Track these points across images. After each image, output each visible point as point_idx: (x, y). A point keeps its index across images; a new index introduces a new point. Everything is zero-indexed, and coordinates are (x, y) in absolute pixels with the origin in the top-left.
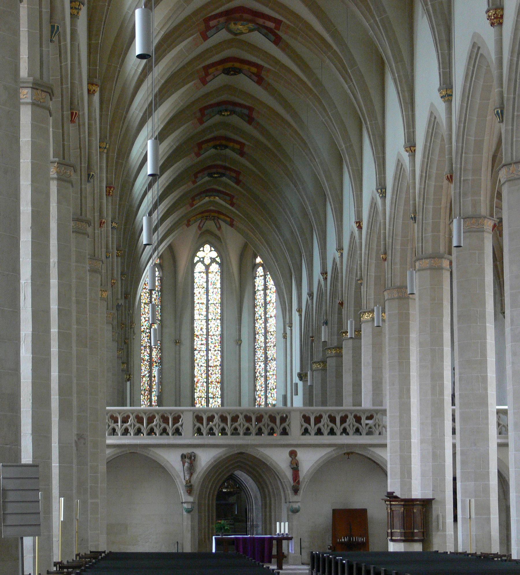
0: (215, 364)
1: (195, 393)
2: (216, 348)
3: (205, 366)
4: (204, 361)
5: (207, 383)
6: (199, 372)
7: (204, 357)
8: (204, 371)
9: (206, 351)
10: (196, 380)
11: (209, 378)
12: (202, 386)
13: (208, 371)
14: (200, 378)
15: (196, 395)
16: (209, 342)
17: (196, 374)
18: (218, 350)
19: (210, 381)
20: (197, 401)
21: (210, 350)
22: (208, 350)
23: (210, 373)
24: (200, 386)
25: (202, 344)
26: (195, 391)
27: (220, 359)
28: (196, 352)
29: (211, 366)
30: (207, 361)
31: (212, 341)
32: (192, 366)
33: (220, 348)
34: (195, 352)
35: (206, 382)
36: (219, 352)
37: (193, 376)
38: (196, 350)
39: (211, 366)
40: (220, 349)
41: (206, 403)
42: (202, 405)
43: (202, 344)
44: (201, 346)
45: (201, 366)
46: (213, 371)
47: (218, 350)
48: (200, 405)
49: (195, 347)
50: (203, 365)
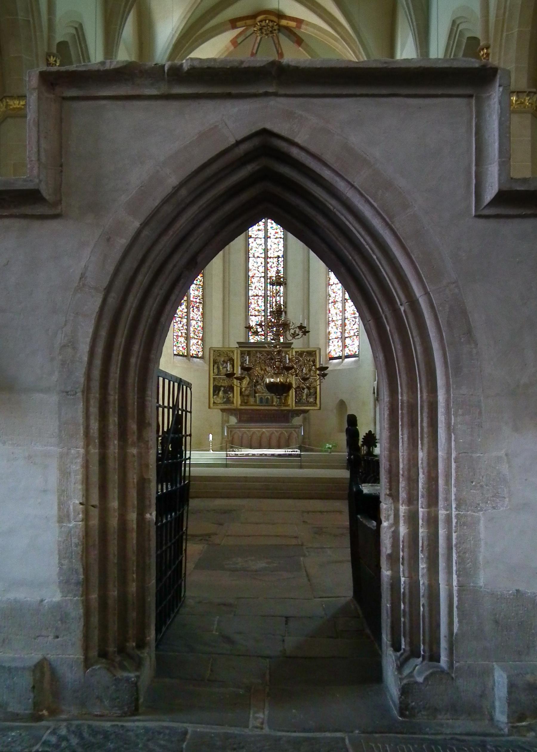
0: (276, 254)
1: (250, 291)
2: (277, 235)
3: (264, 257)
4: (262, 251)
5: (266, 278)
6: (256, 265)
7: (261, 246)
8: (262, 263)
9: (264, 238)
10: (251, 274)
11: (268, 272)
12: (259, 282)
13: (266, 263)
14: (256, 272)
15: (251, 293)
16: (269, 228)
17: (250, 266)
18: (281, 238)
19: (269, 276)
20: (251, 300)
21: (270, 237)
22: (266, 237)
23: (269, 265)
24: (256, 282)
25: (259, 230)
26: (250, 288)
27: (282, 249)
28: (251, 240)
29: (270, 258)
30: (266, 251)
31: (272, 226)
32: (246, 258)
33: (283, 234)
34: (250, 240)
35: (264, 277)
36: (282, 240)
37: (247, 270)
38: (251, 237)
39: (270, 258)
40: (282, 236)
41: (264, 303)
42: (258, 304)
43: (259, 230)
44: (258, 232)
45: (258, 257)
46: (273, 263)
47: (281, 238)
48: (256, 305)
49: (250, 234)
50: (260, 256)
